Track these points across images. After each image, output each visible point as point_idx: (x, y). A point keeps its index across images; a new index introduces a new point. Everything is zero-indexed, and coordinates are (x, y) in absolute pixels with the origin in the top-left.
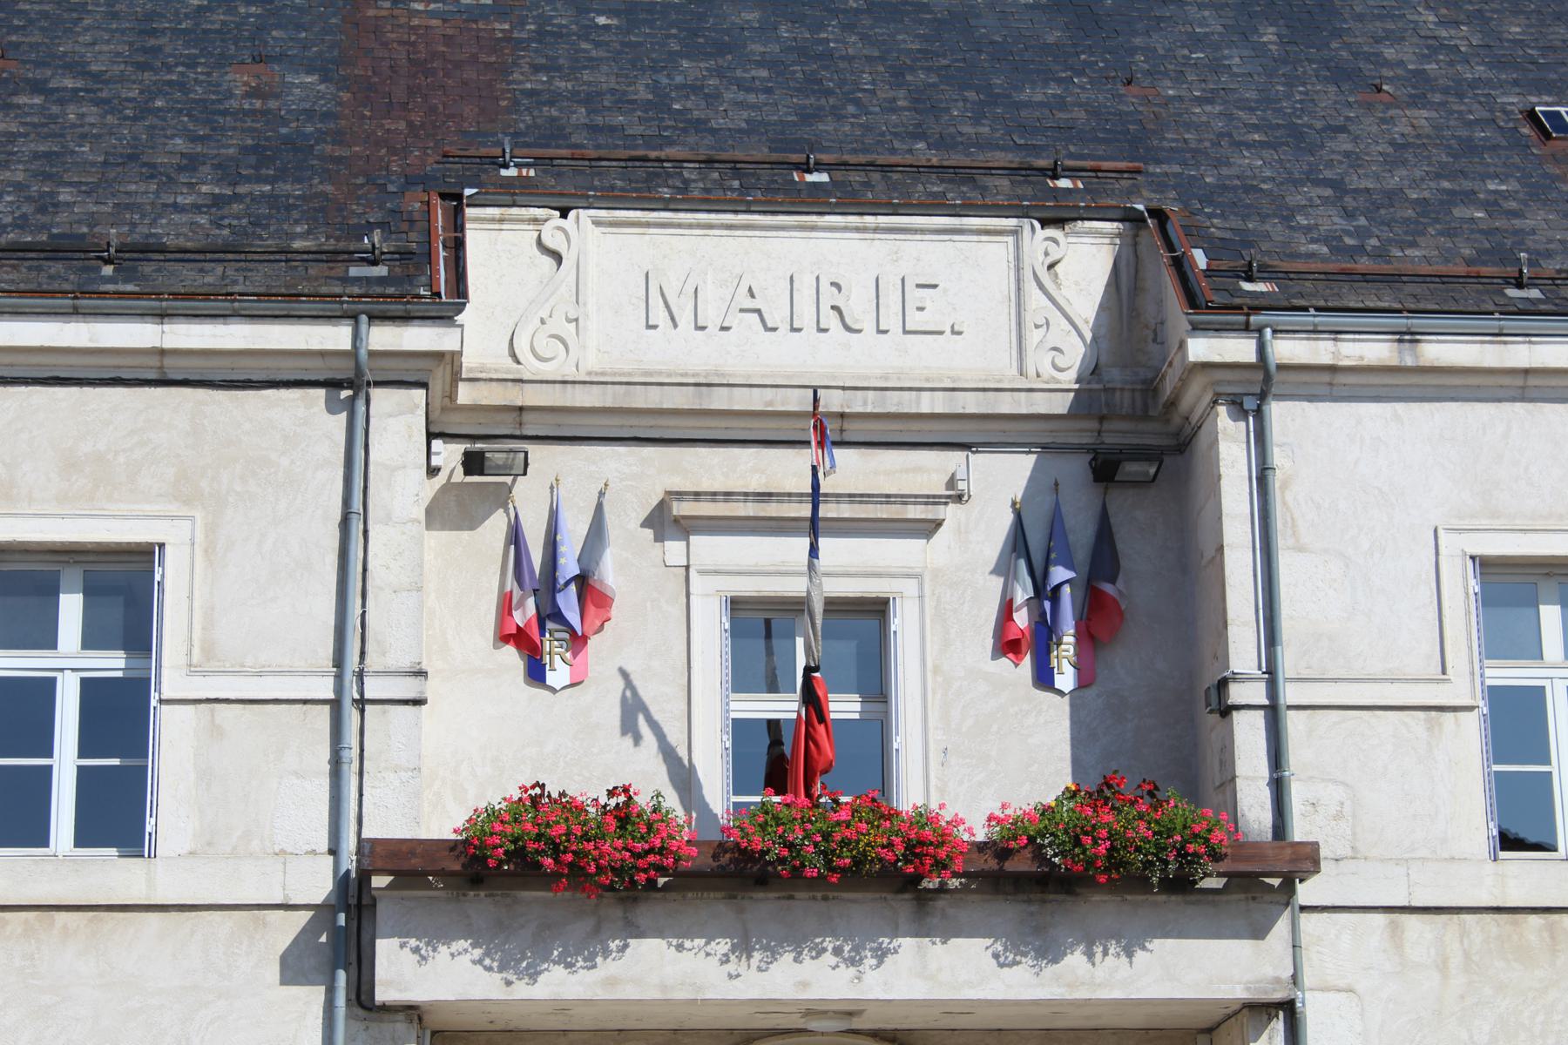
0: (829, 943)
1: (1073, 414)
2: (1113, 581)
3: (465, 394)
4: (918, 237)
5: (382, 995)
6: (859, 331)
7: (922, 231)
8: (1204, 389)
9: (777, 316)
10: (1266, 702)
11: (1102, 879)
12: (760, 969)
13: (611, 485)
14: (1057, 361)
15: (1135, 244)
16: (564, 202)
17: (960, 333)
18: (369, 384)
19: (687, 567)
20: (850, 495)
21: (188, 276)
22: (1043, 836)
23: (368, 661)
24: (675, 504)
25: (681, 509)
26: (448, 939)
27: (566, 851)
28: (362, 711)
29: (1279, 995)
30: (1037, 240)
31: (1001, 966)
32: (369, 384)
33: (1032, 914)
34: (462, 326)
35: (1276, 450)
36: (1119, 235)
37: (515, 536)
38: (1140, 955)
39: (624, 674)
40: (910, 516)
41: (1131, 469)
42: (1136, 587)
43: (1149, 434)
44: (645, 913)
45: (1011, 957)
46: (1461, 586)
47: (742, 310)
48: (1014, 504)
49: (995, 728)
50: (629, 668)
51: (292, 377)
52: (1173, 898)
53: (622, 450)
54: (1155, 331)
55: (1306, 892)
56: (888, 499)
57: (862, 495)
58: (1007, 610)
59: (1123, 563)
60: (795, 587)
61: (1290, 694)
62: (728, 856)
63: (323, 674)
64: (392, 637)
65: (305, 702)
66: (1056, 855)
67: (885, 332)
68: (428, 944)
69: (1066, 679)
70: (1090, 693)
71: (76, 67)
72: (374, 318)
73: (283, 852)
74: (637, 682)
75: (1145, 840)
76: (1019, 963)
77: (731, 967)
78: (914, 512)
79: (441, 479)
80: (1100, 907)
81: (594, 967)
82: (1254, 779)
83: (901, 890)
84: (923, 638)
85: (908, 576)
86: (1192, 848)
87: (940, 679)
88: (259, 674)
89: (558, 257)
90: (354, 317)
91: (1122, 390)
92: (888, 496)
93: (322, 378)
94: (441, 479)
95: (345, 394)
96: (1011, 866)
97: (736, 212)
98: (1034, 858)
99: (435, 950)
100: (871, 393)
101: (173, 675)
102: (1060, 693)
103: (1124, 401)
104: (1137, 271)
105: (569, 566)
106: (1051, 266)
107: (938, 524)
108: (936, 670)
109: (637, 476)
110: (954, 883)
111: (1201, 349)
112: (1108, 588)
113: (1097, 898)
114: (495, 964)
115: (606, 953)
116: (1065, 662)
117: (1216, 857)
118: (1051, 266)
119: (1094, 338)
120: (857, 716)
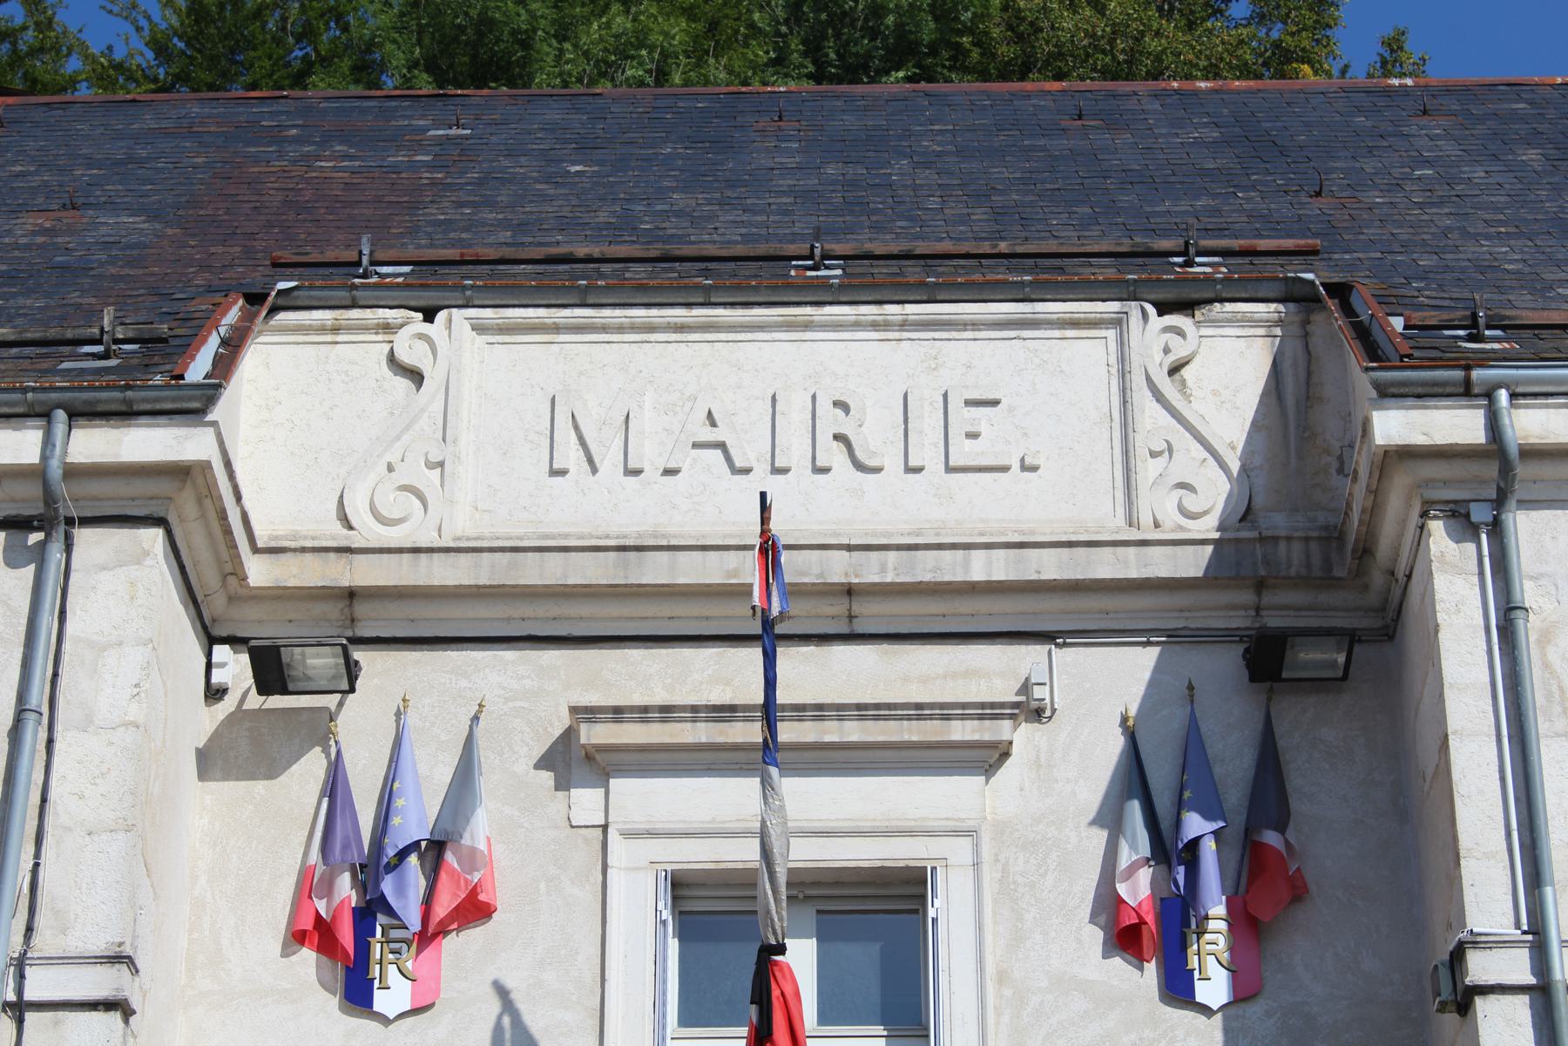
1: (1211, 580)
2: (1281, 828)
3: (259, 572)
6: (878, 470)
7: (975, 325)
10: (1532, 980)
13: (488, 708)
14: (1185, 503)
15: (1306, 335)
16: (428, 298)
17: (1034, 469)
18: (70, 522)
19: (605, 828)
20: (859, 707)
23: (36, 940)
24: (583, 728)
25: (596, 734)
28: (20, 1022)
30: (1151, 333)
32: (70, 522)
34: (214, 424)
35: (1528, 585)
36: (1280, 323)
37: (335, 787)
39: (502, 992)
41: (1309, 657)
47: (696, 445)
48: (1124, 719)
50: (509, 983)
53: (508, 655)
54: (1340, 458)
56: (919, 711)
57: (877, 706)
59: (1295, 804)
67: (918, 470)
69: (1214, 987)
70: (1255, 1009)
72: (81, 414)
78: (961, 731)
79: (228, 705)
84: (980, 928)
87: (1008, 992)
89: (416, 376)
90: (46, 415)
91: (1289, 539)
92: (919, 706)
94: (228, 705)
95: (35, 537)
97: (689, 305)
102: (1205, 1010)
103: (1292, 557)
104: (1309, 373)
105: (413, 824)
106: (1174, 370)
107: (1000, 753)
108: (1002, 977)
109: (530, 692)
111: (1394, 426)
112: (1271, 838)
118: (1174, 370)
119: (1244, 469)
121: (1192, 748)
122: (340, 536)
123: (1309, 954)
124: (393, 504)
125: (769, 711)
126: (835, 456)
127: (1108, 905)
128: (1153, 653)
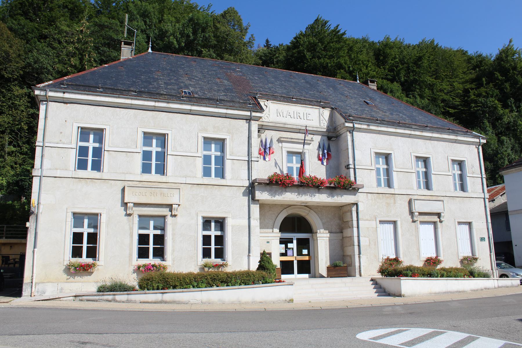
5: (257, 198)
9: (292, 116)
21: (228, 104)
30: (322, 110)
37: (262, 141)
41: (333, 139)
42: (332, 153)
43: (334, 135)
44: (287, 189)
46: (373, 155)
55: (360, 190)
58: (319, 155)
60: (301, 151)
61: (356, 167)
69: (325, 164)
71: (196, 77)
72: (253, 111)
80: (338, 191)
101: (228, 156)
103: (332, 130)
107: (310, 144)
109: (276, 135)
123: (331, 161)
126: (298, 117)
128: (320, 137)
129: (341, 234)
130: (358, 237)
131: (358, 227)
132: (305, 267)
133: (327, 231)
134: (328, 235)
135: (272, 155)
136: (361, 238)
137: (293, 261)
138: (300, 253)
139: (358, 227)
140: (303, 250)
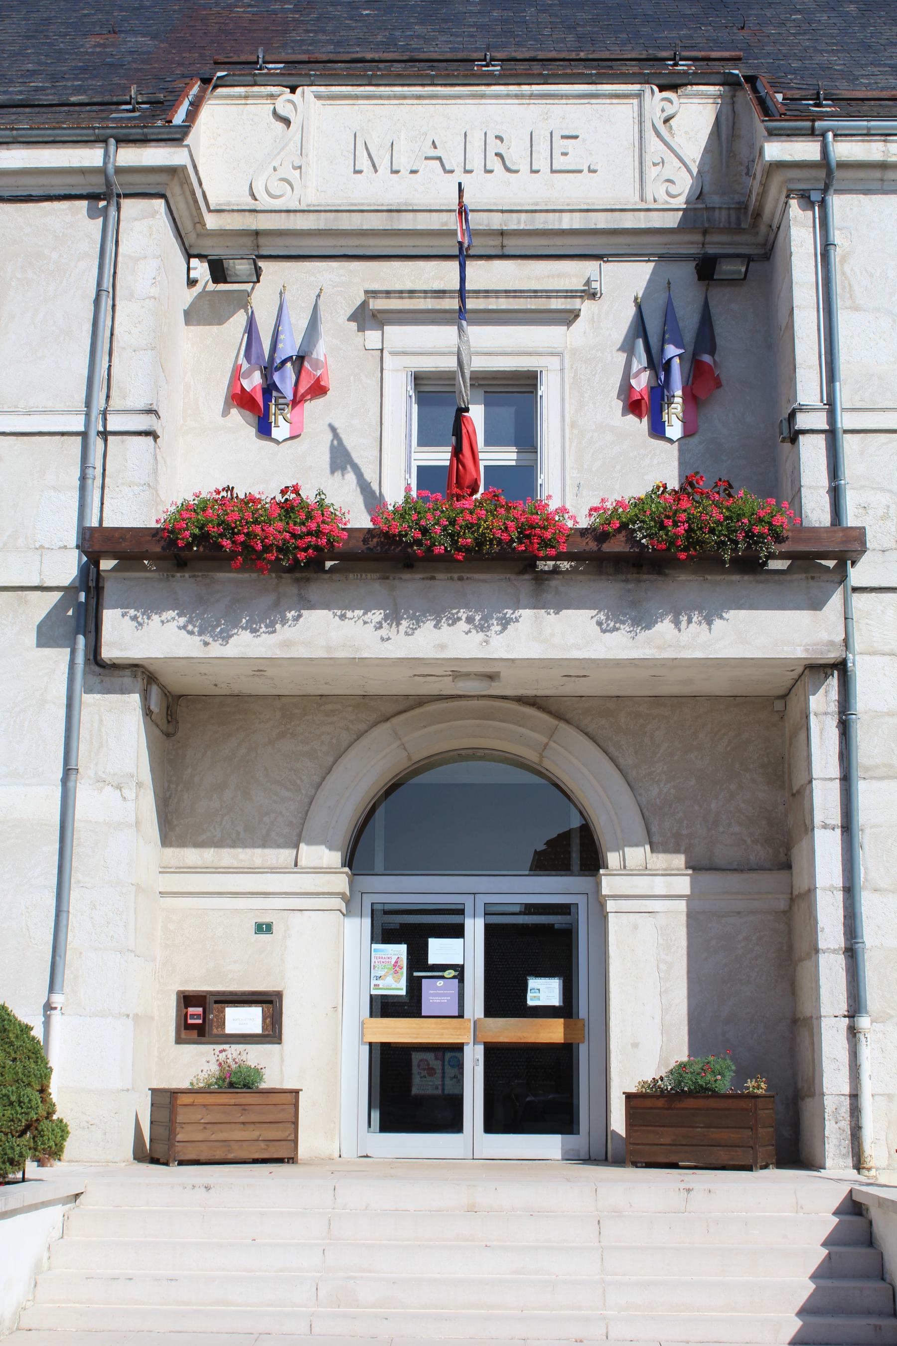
0: (463, 614)
1: (682, 228)
2: (712, 353)
3: (212, 222)
4: (564, 101)
5: (108, 653)
6: (517, 172)
8: (780, 192)
10: (827, 427)
11: (683, 556)
12: (407, 634)
14: (669, 190)
15: (733, 103)
16: (292, 81)
17: (595, 171)
18: (119, 196)
19: (382, 350)
20: (506, 291)
22: (634, 523)
23: (111, 402)
24: (371, 301)
25: (377, 304)
26: (159, 608)
27: (239, 533)
28: (106, 441)
29: (833, 655)
30: (656, 101)
31: (604, 631)
32: (119, 196)
33: (629, 591)
34: (187, 146)
35: (837, 233)
36: (720, 96)
37: (251, 328)
38: (717, 623)
39: (333, 429)
40: (553, 307)
41: (727, 268)
43: (744, 244)
44: (314, 591)
45: (612, 624)
47: (426, 158)
48: (636, 299)
49: (618, 467)
50: (336, 425)
51: (62, 192)
52: (746, 578)
53: (334, 264)
55: (857, 575)
56: (536, 294)
57: (515, 291)
59: (719, 342)
61: (845, 421)
62: (375, 540)
63: (77, 413)
64: (132, 385)
65: (63, 434)
66: (644, 537)
67: (537, 172)
68: (143, 614)
69: (675, 430)
70: (695, 440)
72: (123, 141)
73: (42, 547)
74: (343, 435)
75: (719, 523)
76: (618, 629)
77: (383, 632)
78: (556, 304)
80: (686, 585)
81: (274, 632)
82: (816, 488)
83: (522, 572)
85: (552, 354)
86: (758, 529)
87: (576, 431)
88: (28, 413)
89: (287, 122)
90: (105, 141)
91: (720, 208)
92: (536, 291)
93: (84, 192)
95: (102, 204)
96: (609, 547)
97: (423, 85)
98: (627, 541)
99: (149, 618)
100: (523, 215)
102: (670, 441)
103: (721, 217)
104: (734, 123)
105: (289, 347)
106: (666, 121)
108: (573, 424)
110: (565, 565)
111: (775, 150)
112: (706, 358)
113: (683, 577)
114: (196, 629)
115: (284, 621)
116: (674, 417)
117: (779, 539)
118: (666, 121)
119: (699, 172)
120: (514, 463)
121: (669, 314)
122: (249, 203)
123: (722, 416)
124: (277, 187)
125: (462, 293)
126: (495, 164)
127: (626, 389)
128: (652, 265)
129: (769, 880)
130: (850, 890)
131: (848, 827)
132: (537, 1092)
133: (679, 860)
134: (683, 884)
135: (311, 407)
136: (867, 902)
137: (458, 1048)
138: (505, 997)
139: (848, 827)
140: (533, 983)
